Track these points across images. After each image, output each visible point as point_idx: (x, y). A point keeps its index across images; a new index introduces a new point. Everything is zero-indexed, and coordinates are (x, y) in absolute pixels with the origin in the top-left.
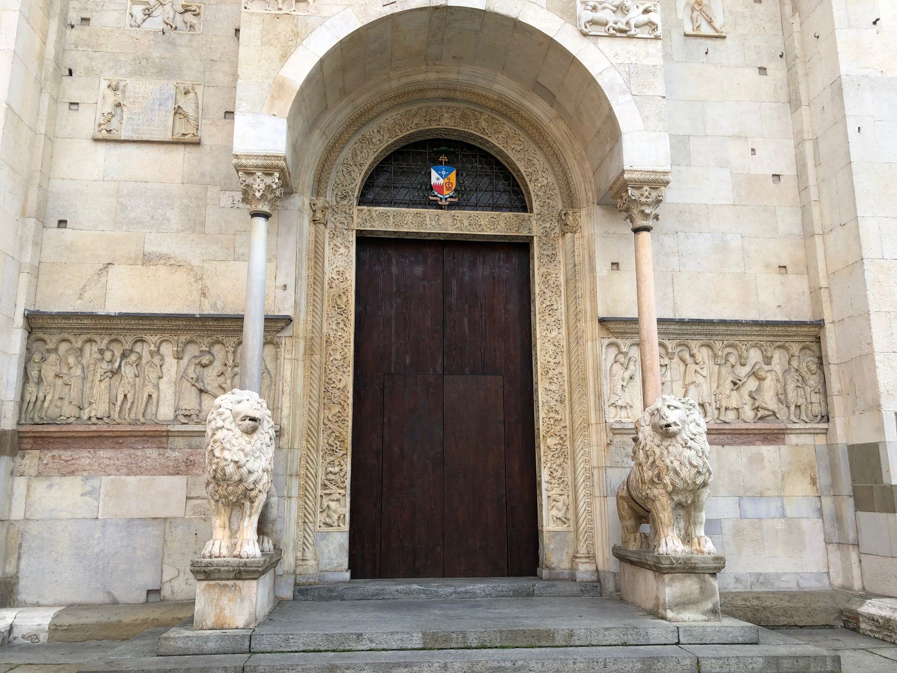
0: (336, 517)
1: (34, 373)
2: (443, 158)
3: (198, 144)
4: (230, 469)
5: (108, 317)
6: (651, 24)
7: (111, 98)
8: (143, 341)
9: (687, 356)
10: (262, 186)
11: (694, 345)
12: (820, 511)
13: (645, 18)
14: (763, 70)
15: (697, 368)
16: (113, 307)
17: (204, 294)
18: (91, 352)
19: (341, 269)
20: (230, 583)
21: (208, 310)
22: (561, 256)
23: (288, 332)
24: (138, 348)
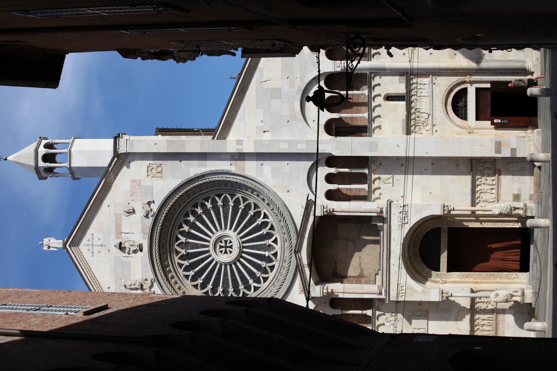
0: (516, 276)
3: (428, 311)
4: (505, 298)
5: (471, 328)
9: (479, 192)
12: (517, 162)
15: (482, 190)
19: (457, 276)
20: (525, 297)
23: (474, 289)
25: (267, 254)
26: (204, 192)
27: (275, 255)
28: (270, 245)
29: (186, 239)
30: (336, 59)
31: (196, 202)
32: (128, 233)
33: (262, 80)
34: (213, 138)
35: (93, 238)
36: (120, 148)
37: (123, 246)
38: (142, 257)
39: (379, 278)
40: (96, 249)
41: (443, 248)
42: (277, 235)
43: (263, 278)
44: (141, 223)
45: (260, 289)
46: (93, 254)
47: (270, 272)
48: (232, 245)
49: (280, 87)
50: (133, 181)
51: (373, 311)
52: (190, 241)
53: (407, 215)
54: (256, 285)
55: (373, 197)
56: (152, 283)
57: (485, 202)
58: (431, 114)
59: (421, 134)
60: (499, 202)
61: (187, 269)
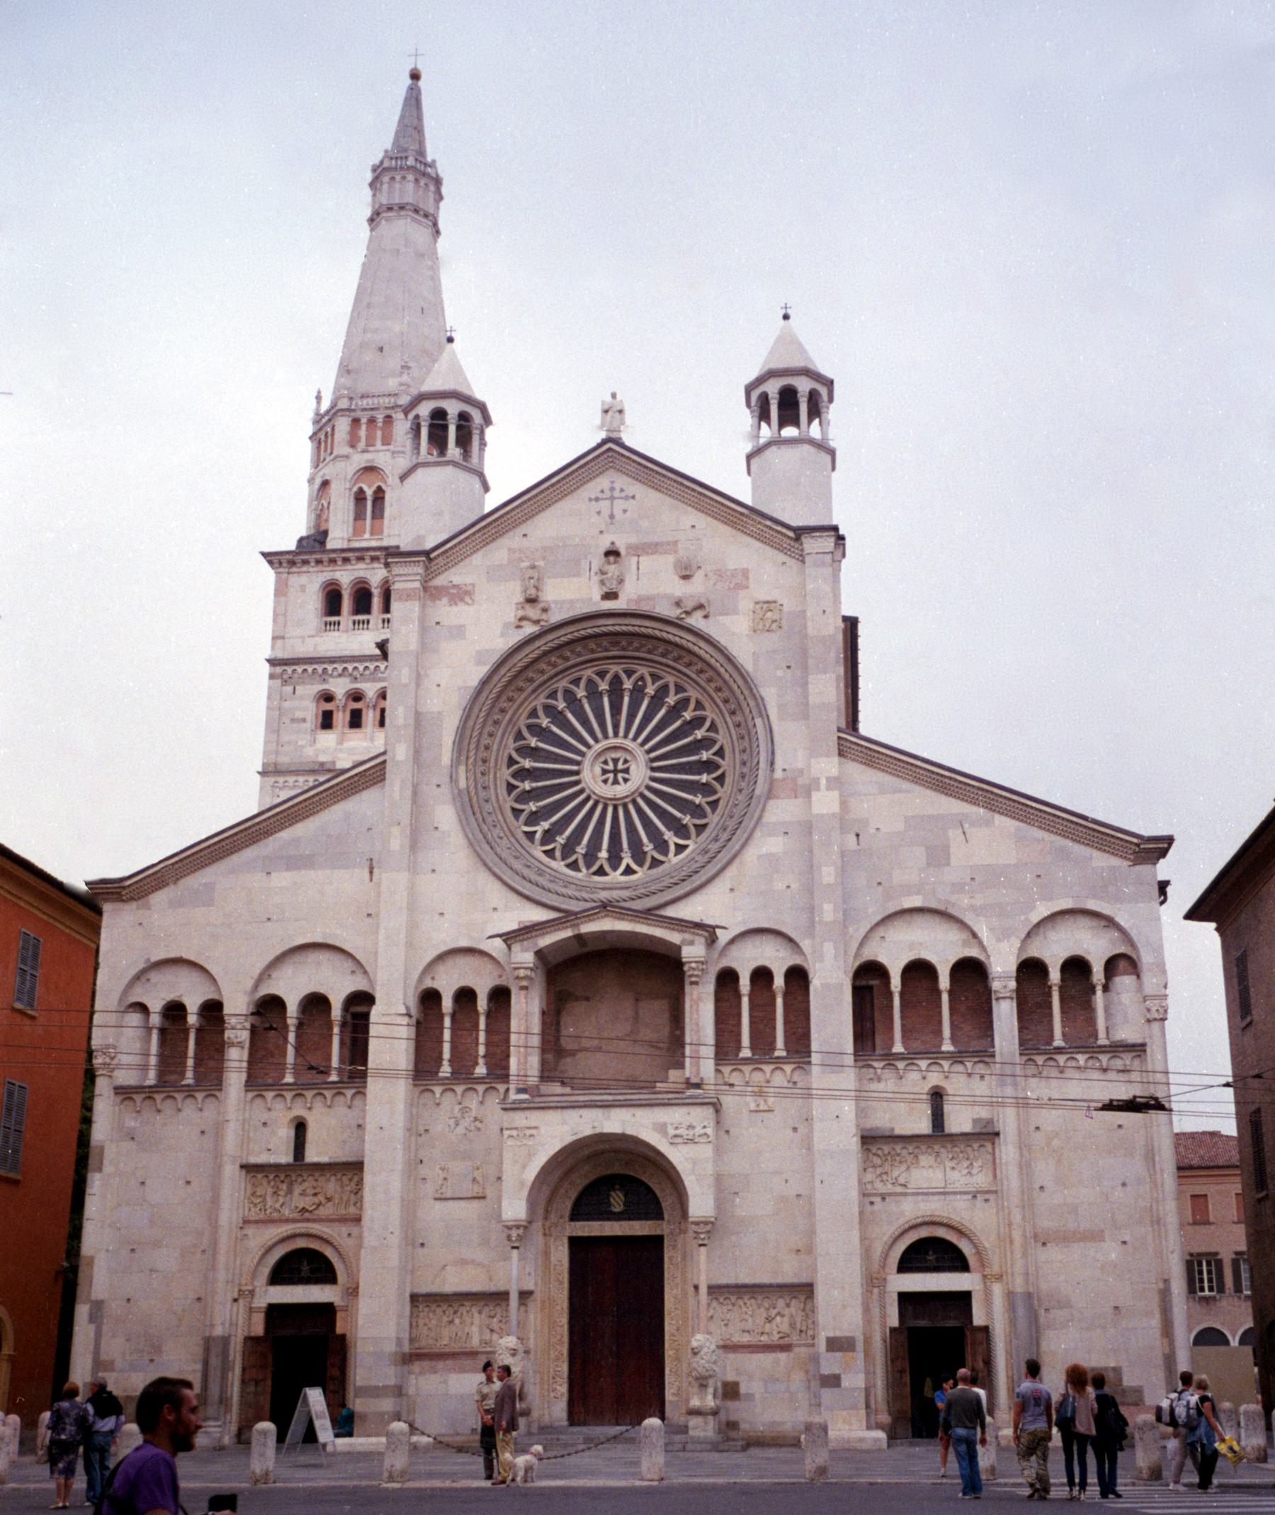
1: (414, 1324)
3: (484, 1198)
5: (447, 1295)
6: (705, 1134)
7: (442, 1175)
8: (463, 1305)
11: (746, 1298)
12: (809, 1387)
13: (702, 1131)
14: (795, 1129)
16: (448, 1288)
18: (439, 1311)
21: (493, 1289)
22: (679, 1246)
24: (461, 1308)
25: (604, 854)
26: (728, 719)
27: (601, 872)
28: (621, 859)
30: (1018, 979)
31: (707, 705)
33: (966, 826)
34: (839, 730)
35: (627, 498)
36: (812, 541)
37: (612, 559)
38: (591, 599)
39: (557, 1088)
41: (621, 1226)
42: (641, 874)
43: (554, 849)
45: (530, 844)
46: (594, 503)
49: (953, 860)
50: (745, 573)
51: (484, 1078)
52: (626, 700)
54: (538, 836)
55: (726, 1070)
56: (537, 622)
58: (908, 1191)
59: (865, 1170)
60: (721, 1351)
61: (570, 697)
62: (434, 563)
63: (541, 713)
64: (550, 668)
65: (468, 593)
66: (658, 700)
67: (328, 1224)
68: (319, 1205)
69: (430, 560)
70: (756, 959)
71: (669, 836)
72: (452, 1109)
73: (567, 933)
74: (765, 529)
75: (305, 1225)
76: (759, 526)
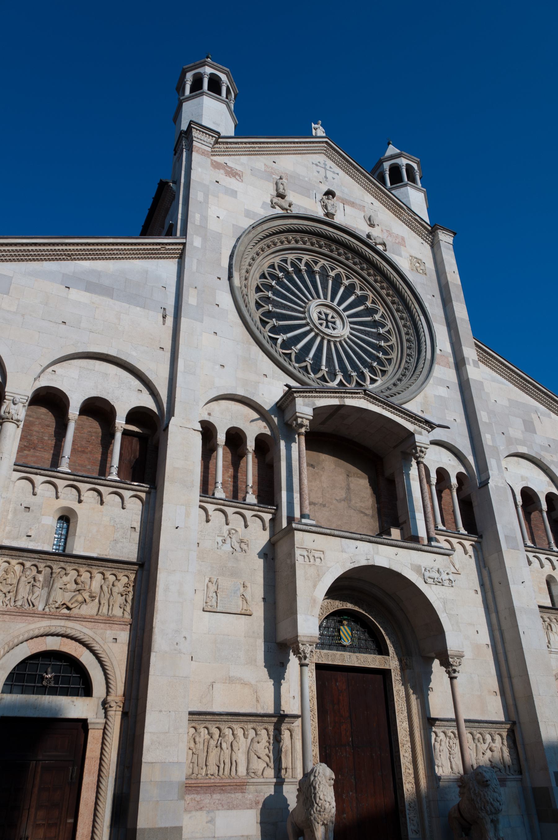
2: (345, 622)
6: (450, 580)
7: (213, 588)
10: (309, 652)
16: (216, 708)
17: (258, 701)
28: (335, 375)
29: (333, 277)
32: (344, 210)
33: (539, 414)
35: (334, 172)
36: (443, 235)
40: (322, 171)
44: (357, 228)
47: (300, 366)
48: (329, 328)
50: (403, 239)
51: (255, 505)
53: (438, 583)
54: (279, 341)
56: (287, 210)
57: (450, 751)
62: (218, 146)
63: (277, 268)
64: (286, 242)
65: (237, 174)
66: (350, 290)
67: (89, 625)
68: (82, 603)
69: (217, 142)
70: (438, 462)
71: (366, 371)
72: (221, 529)
73: (335, 402)
74: (413, 221)
75: (62, 623)
76: (410, 218)
